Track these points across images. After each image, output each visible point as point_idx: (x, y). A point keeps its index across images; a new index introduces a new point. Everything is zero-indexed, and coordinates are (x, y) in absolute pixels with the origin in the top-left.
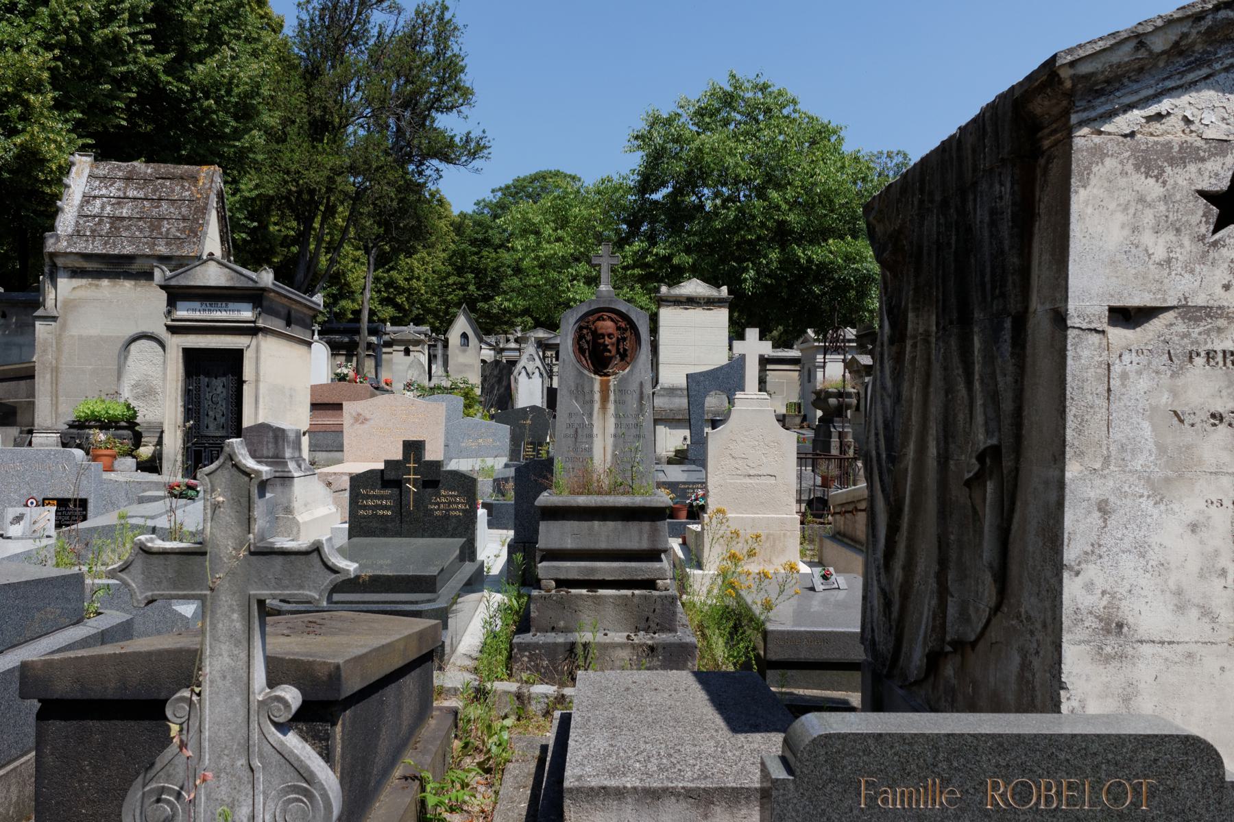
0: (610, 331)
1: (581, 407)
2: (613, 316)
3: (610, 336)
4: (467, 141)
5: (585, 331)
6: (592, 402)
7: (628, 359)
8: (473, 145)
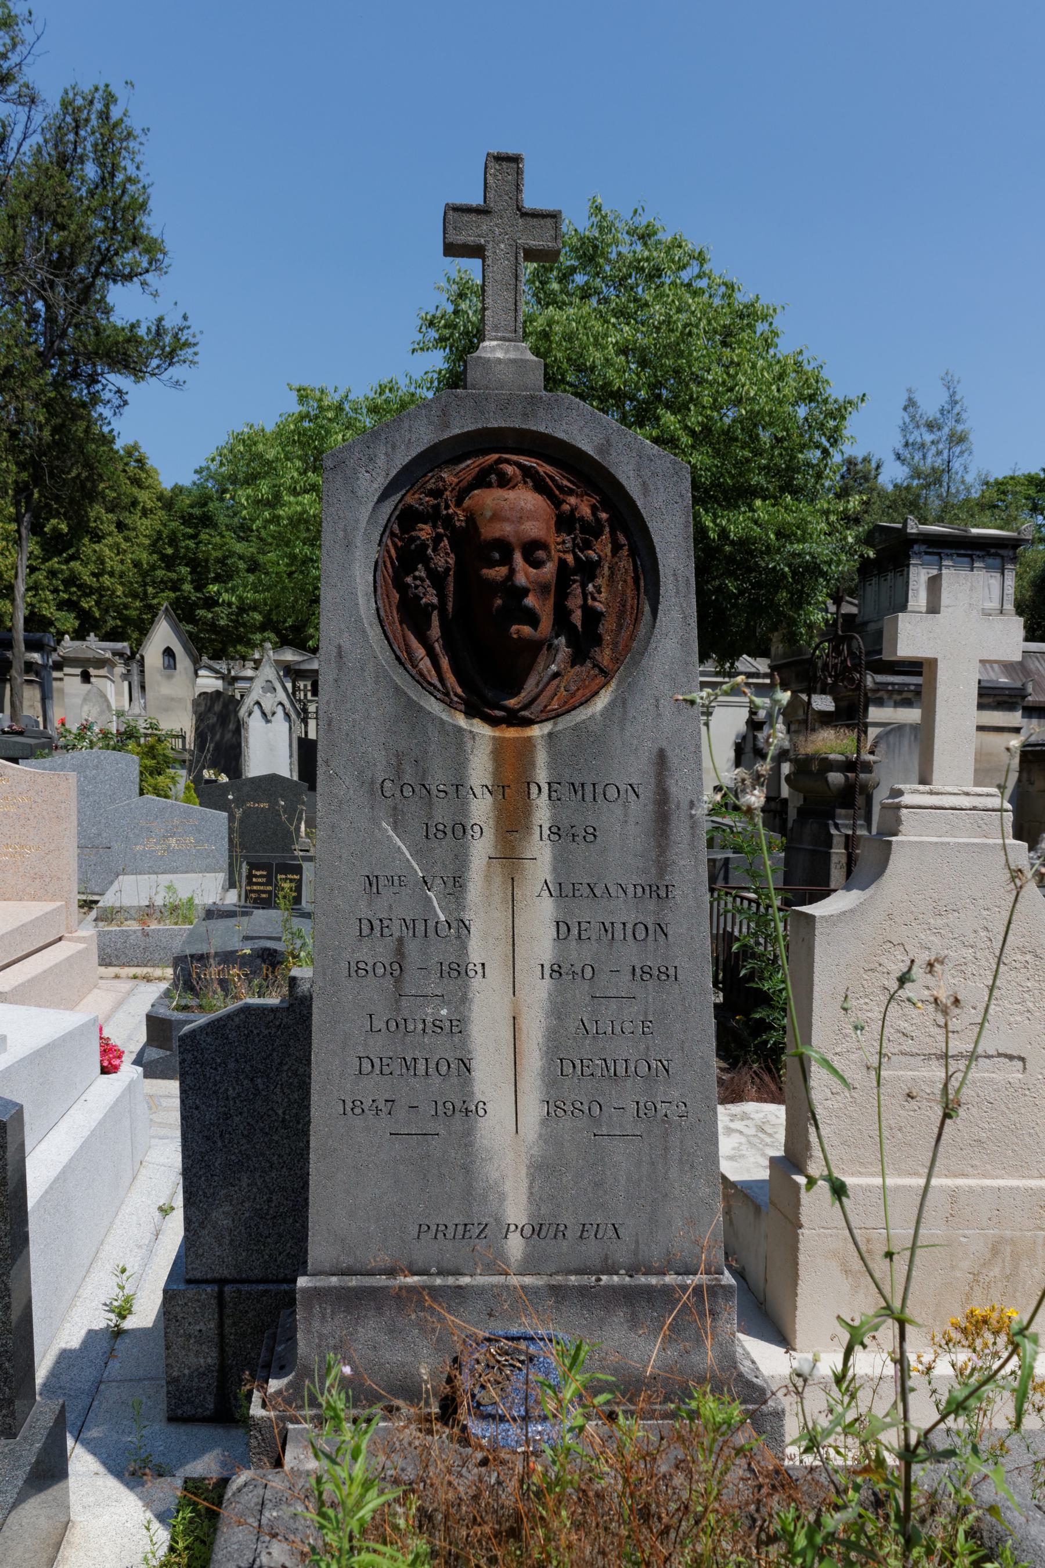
0: (534, 529)
1: (417, 854)
2: (544, 469)
3: (532, 549)
4: (158, 334)
5: (425, 532)
6: (460, 830)
7: (604, 656)
8: (168, 339)
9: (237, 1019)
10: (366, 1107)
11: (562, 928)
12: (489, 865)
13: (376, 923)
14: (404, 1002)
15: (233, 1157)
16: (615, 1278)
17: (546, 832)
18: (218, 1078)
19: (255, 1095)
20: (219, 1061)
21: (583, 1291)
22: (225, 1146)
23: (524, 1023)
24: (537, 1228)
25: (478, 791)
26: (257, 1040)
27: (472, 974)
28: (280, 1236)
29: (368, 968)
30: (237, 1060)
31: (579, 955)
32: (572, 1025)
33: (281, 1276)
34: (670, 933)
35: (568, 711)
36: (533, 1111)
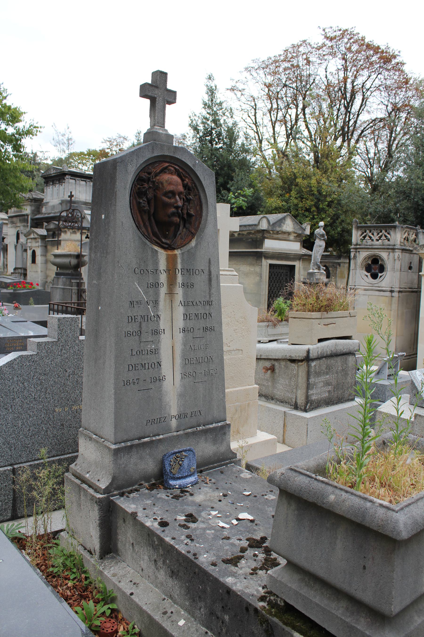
1: (146, 293)
9: (18, 360)
10: (131, 382)
11: (186, 317)
12: (165, 296)
13: (133, 317)
14: (142, 344)
15: (16, 415)
16: (201, 427)
17: (180, 285)
18: (10, 384)
19: (24, 389)
20: (11, 377)
21: (193, 433)
22: (13, 411)
23: (175, 348)
24: (180, 416)
25: (162, 272)
26: (25, 368)
27: (161, 333)
28: (33, 443)
29: (131, 333)
30: (17, 377)
31: (190, 324)
32: (188, 347)
33: (33, 459)
34: (212, 316)
35: (184, 246)
36: (178, 377)
